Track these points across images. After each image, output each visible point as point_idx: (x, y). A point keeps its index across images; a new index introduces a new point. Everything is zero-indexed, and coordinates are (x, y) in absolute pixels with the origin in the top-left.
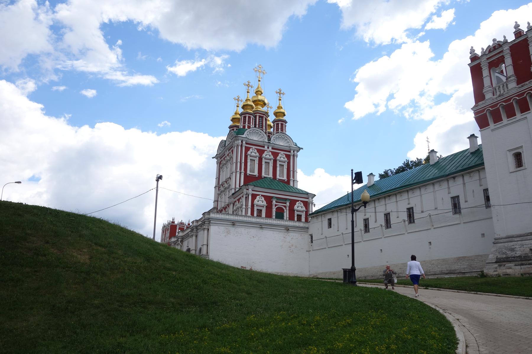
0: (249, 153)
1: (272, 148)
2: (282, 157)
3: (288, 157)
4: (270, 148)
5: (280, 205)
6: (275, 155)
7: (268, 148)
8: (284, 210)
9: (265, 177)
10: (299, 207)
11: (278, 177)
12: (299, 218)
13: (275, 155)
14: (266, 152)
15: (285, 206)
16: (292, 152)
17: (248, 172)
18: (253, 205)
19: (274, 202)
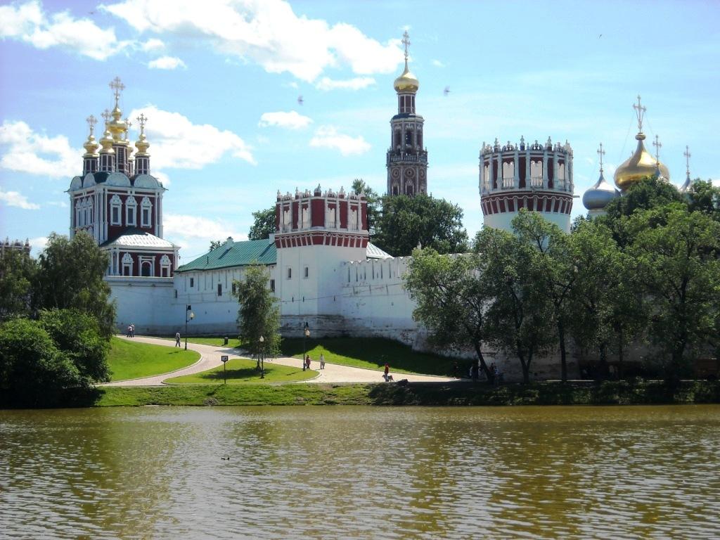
0: (112, 201)
1: (136, 193)
2: (146, 203)
3: (152, 200)
4: (134, 194)
5: (146, 261)
6: (139, 200)
7: (131, 193)
8: (149, 265)
9: (129, 226)
10: (165, 262)
11: (142, 224)
12: (165, 275)
13: (139, 200)
14: (129, 198)
15: (151, 261)
16: (157, 194)
17: (112, 223)
18: (120, 264)
19: (140, 258)
